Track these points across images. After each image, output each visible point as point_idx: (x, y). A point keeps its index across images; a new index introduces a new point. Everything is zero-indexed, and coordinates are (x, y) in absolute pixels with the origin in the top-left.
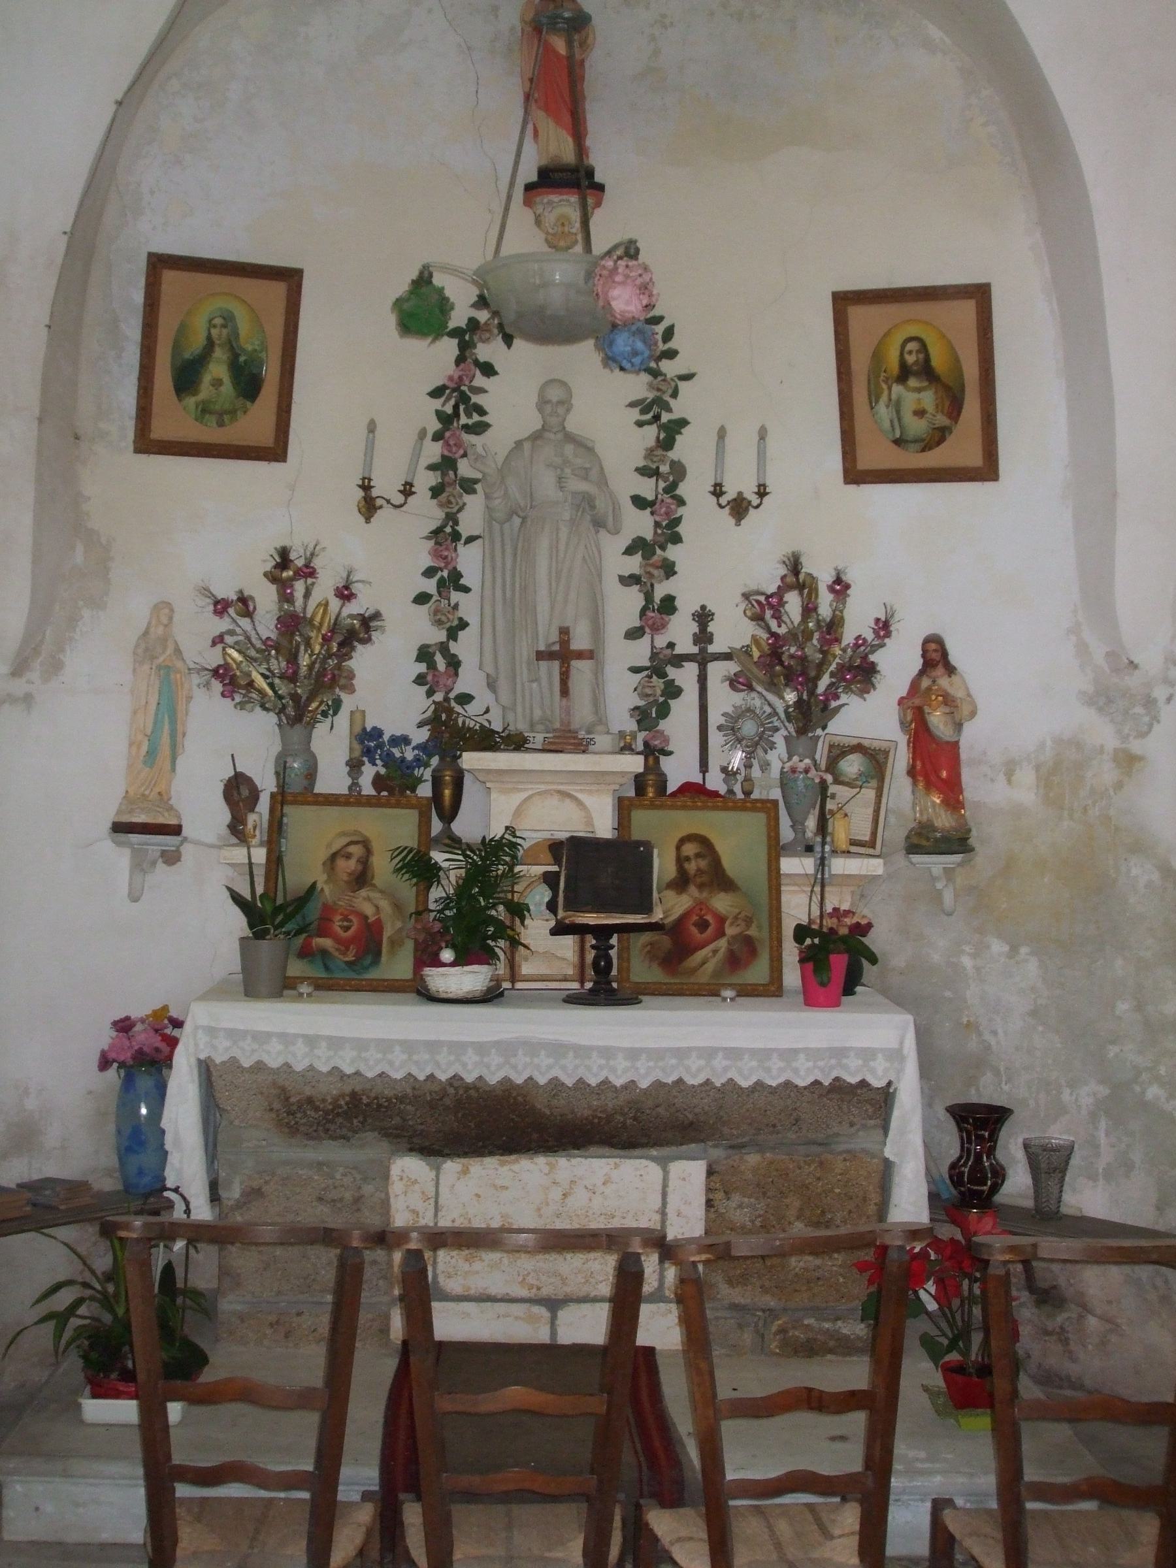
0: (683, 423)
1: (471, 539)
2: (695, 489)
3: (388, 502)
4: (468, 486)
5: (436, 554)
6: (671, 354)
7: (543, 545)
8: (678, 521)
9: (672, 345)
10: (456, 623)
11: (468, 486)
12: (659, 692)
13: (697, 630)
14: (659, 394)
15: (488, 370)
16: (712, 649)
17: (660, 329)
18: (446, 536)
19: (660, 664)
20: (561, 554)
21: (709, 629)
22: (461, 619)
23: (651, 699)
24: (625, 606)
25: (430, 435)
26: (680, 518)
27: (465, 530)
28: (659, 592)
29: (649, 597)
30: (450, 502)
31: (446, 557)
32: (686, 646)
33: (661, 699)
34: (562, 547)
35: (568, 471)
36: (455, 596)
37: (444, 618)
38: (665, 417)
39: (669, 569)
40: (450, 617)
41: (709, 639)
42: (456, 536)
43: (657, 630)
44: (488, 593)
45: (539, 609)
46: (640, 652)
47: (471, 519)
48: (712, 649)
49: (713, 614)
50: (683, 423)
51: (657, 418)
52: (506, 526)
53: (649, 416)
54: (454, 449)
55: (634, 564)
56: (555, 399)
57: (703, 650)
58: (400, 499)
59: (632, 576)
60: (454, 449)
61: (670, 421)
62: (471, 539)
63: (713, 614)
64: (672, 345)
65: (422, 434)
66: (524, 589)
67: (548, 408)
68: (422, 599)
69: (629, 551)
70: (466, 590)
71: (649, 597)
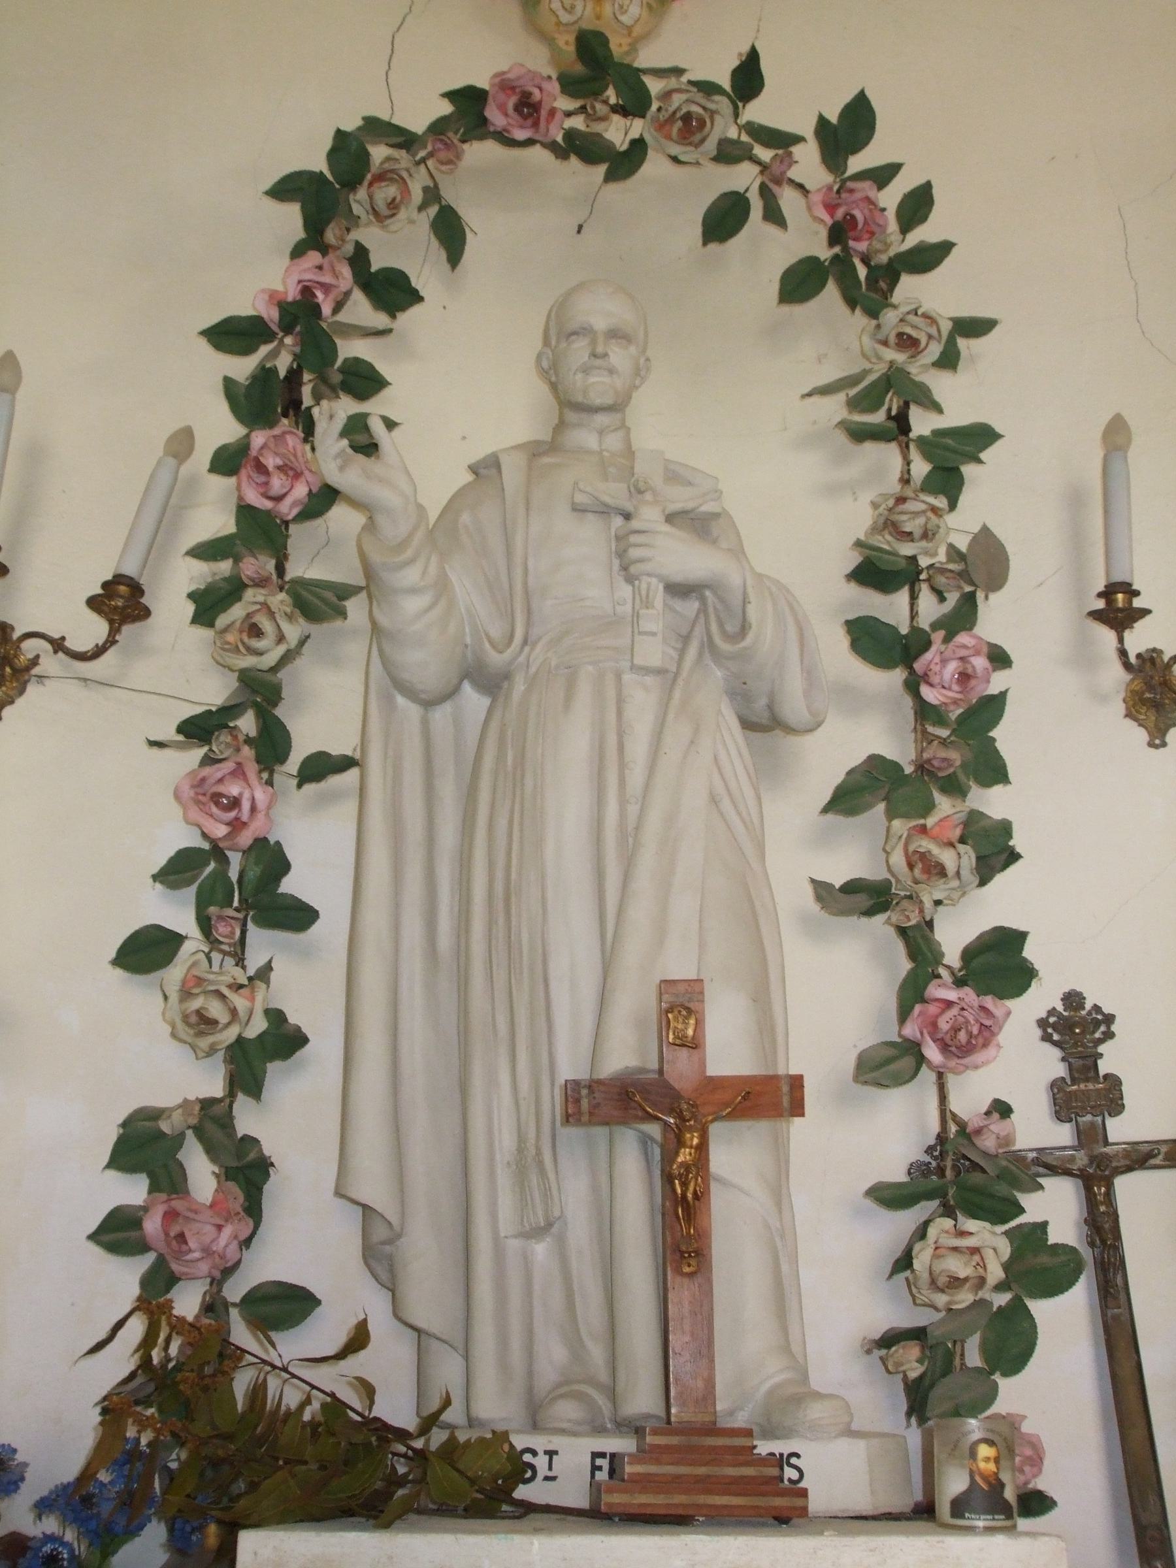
0: (981, 436)
1: (320, 768)
2: (1034, 618)
3: (58, 645)
4: (318, 604)
5: (205, 796)
6: (928, 258)
7: (569, 750)
8: (993, 706)
9: (926, 233)
10: (258, 1026)
11: (318, 604)
12: (995, 1273)
13: (1059, 1070)
14: (900, 357)
15: (393, 292)
16: (1121, 1130)
17: (890, 198)
18: (246, 730)
19: (961, 1176)
20: (636, 777)
21: (1104, 1067)
22: (276, 1017)
23: (965, 1298)
24: (838, 991)
25: (203, 455)
26: (1003, 695)
27: (309, 735)
28: (954, 936)
29: (918, 942)
30: (255, 631)
31: (235, 803)
32: (1037, 1128)
33: (1002, 1299)
34: (638, 749)
35: (650, 516)
36: (263, 944)
37: (216, 1010)
38: (922, 424)
39: (994, 850)
40: (239, 1001)
41: (1111, 1097)
42: (272, 745)
43: (967, 1050)
44: (375, 918)
45: (559, 967)
46: (896, 1132)
47: (325, 708)
48: (1121, 1130)
49: (1109, 1019)
50: (981, 436)
51: (901, 423)
52: (441, 715)
53: (878, 417)
54: (277, 483)
55: (851, 856)
56: (600, 324)
57: (1091, 1137)
58: (94, 629)
59: (852, 887)
60: (277, 483)
61: (937, 433)
62: (320, 768)
63: (1109, 1019)
64: (926, 233)
65: (181, 443)
66: (505, 900)
67: (579, 351)
68: (145, 951)
69: (846, 799)
70: (300, 916)
71: (918, 942)
